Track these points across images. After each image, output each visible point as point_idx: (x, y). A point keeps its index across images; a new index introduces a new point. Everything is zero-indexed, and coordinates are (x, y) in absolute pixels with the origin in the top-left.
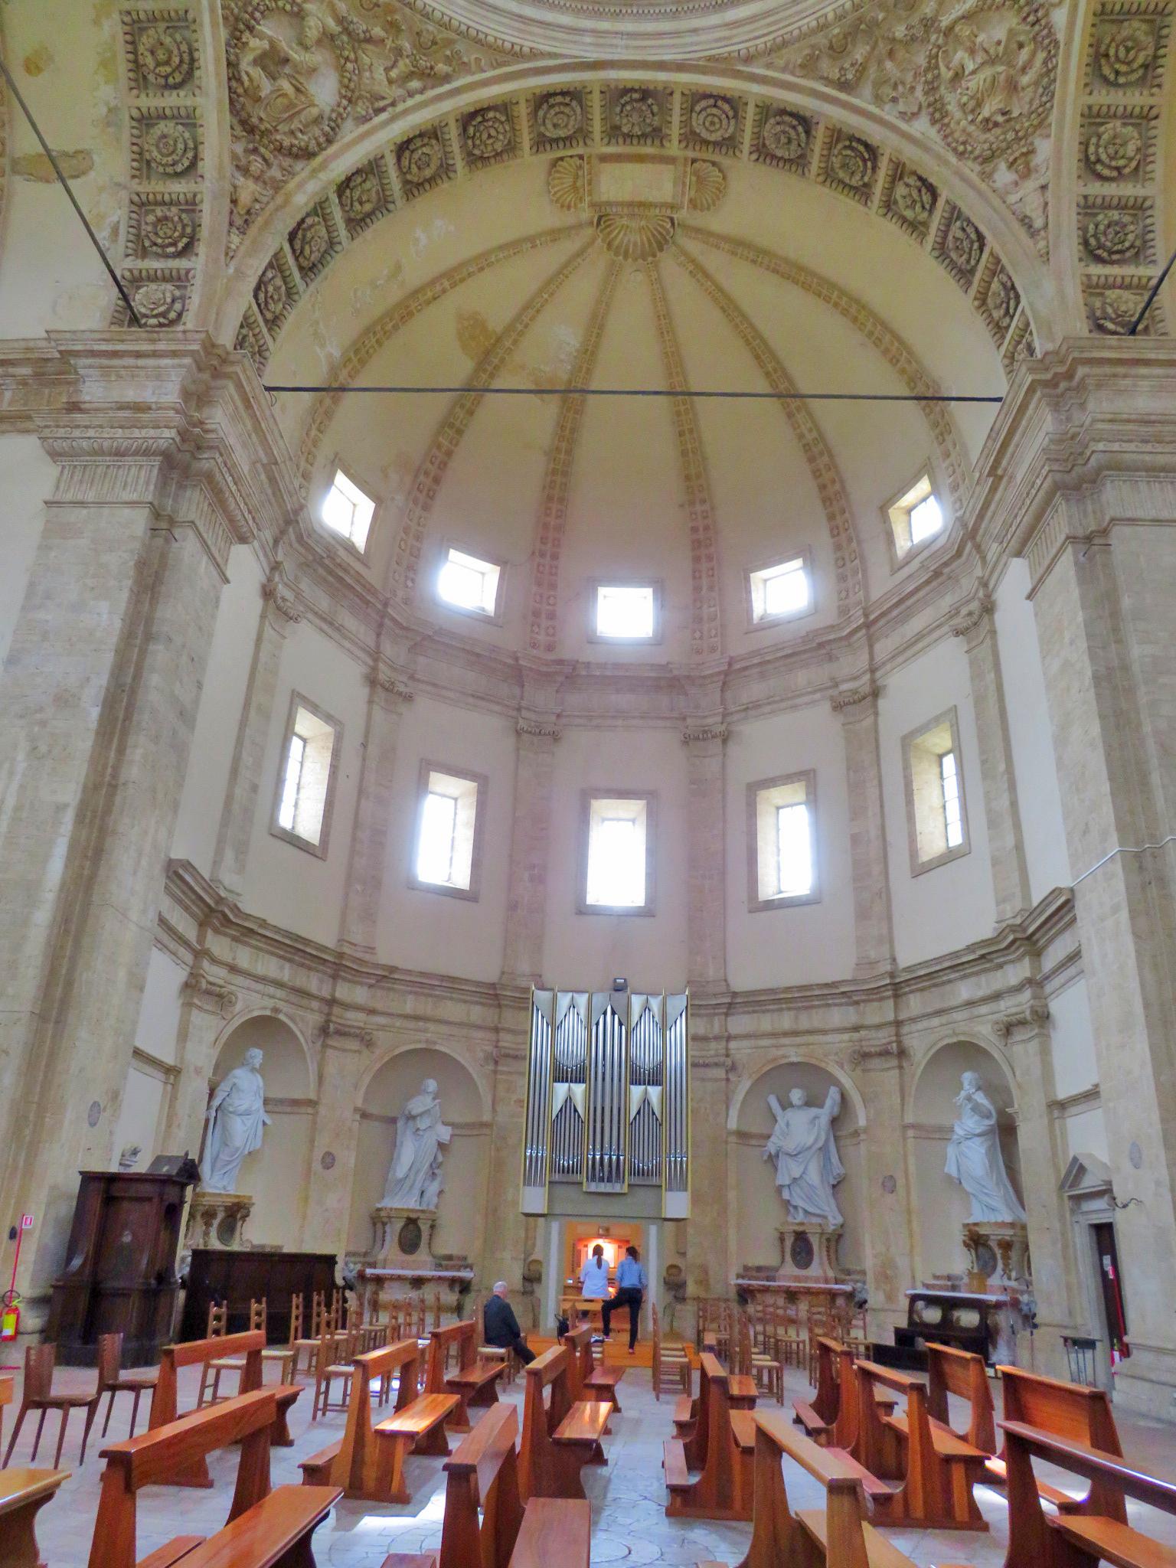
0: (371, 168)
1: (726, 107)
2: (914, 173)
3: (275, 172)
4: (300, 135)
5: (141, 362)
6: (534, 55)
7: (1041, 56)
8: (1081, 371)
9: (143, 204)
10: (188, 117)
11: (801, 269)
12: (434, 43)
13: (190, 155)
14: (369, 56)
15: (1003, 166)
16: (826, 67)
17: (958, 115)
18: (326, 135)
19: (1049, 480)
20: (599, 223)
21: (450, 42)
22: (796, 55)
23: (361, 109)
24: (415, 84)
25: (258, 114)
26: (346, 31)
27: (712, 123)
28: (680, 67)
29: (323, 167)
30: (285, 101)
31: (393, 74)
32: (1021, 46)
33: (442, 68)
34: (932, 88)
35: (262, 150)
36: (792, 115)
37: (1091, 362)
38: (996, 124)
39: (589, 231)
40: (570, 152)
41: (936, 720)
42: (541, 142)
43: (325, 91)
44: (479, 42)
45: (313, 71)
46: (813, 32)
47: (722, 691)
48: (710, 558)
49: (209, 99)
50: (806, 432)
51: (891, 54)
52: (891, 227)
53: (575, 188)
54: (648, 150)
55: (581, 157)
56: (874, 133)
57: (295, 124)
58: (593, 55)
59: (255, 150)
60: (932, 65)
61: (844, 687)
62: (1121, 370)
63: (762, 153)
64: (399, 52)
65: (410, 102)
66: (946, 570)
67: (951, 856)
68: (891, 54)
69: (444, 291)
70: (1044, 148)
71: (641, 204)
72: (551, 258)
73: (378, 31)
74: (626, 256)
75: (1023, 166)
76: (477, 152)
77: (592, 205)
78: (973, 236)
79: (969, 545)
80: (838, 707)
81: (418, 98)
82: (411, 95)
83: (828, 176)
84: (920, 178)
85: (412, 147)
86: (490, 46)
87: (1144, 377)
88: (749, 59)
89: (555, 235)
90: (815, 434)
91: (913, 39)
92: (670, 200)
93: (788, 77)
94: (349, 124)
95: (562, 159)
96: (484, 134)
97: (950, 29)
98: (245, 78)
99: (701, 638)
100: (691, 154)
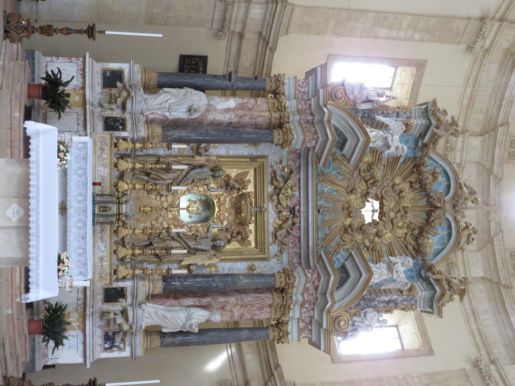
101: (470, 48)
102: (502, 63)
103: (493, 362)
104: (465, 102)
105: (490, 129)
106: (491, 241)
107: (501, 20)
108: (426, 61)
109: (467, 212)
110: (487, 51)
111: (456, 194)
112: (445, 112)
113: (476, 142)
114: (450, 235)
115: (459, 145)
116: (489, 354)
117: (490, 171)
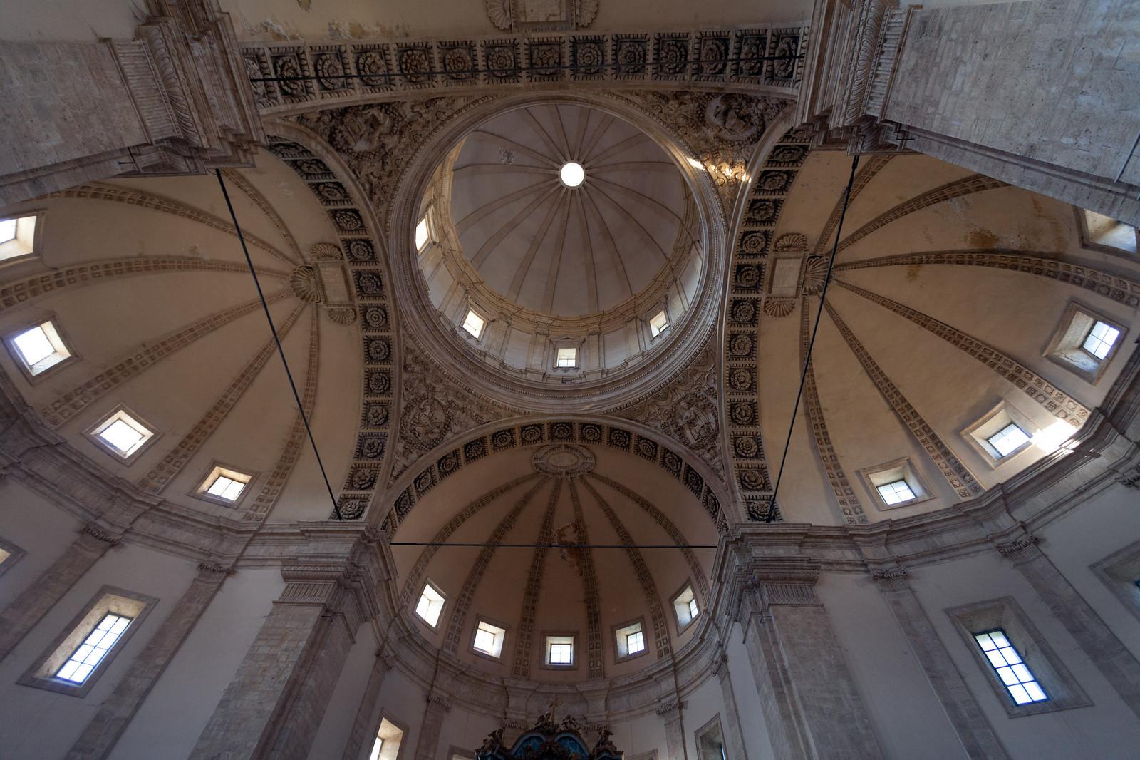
0: (327, 172)
1: (384, 322)
2: (387, 411)
3: (323, 127)
4: (340, 135)
5: (229, 92)
6: (387, 237)
7: (436, 436)
8: (374, 544)
9: (298, 55)
10: (348, 84)
11: (318, 367)
12: (385, 193)
13: (331, 87)
14: (378, 165)
15: (402, 445)
16: (410, 357)
17: (411, 417)
18: (341, 148)
19: (338, 574)
20: (308, 267)
21: (386, 200)
22: (410, 344)
23: (354, 163)
24: (367, 186)
25: (348, 118)
26: (386, 153)
27: (375, 318)
28: (395, 300)
29: (328, 152)
30: (357, 131)
31: (371, 177)
32: (438, 427)
33: (375, 197)
34: (414, 401)
35: (334, 121)
36: (390, 352)
37: (379, 545)
38: (414, 434)
39: (301, 262)
40: (344, 254)
41: (139, 597)
42: (348, 243)
43: (361, 146)
44: (388, 213)
45: (370, 141)
46: (419, 348)
47: (29, 450)
48: (115, 380)
49: (357, 95)
50: (229, 397)
51: (420, 381)
52: (361, 411)
53: (325, 255)
54: (354, 290)
55: (342, 258)
56: (395, 390)
57: (346, 134)
58: (391, 262)
59: (333, 117)
60: (424, 398)
61: (100, 522)
62: (379, 555)
63: (368, 341)
64: (380, 178)
65: (360, 186)
66: (224, 531)
67: (69, 690)
68: (420, 381)
69: (246, 191)
70: (414, 456)
71: (323, 286)
72: (279, 243)
73: (387, 168)
74: (291, 282)
75: (405, 454)
76: (338, 215)
77: (316, 264)
78: (379, 451)
79: (251, 535)
80: (86, 531)
81: (362, 189)
82: (363, 185)
83: (369, 374)
84: (387, 416)
85: (340, 189)
86: (386, 217)
87: (378, 563)
88: (404, 327)
89: (294, 245)
90: (231, 403)
91: (427, 387)
92: (329, 300)
93: (402, 344)
94: (346, 157)
95: (339, 250)
96: (345, 217)
97: (435, 399)
98: (367, 111)
99: (56, 409)
100: (357, 309)
101: (448, 709)
102: (461, 682)
103: (660, 701)
104: (484, 711)
105: (506, 692)
106: (581, 693)
107: (432, 686)
108: (450, 746)
109: (556, 722)
110: (451, 695)
111: (542, 732)
112: (485, 741)
113: (513, 702)
114: (571, 739)
115: (514, 716)
116: (656, 702)
117: (534, 691)
